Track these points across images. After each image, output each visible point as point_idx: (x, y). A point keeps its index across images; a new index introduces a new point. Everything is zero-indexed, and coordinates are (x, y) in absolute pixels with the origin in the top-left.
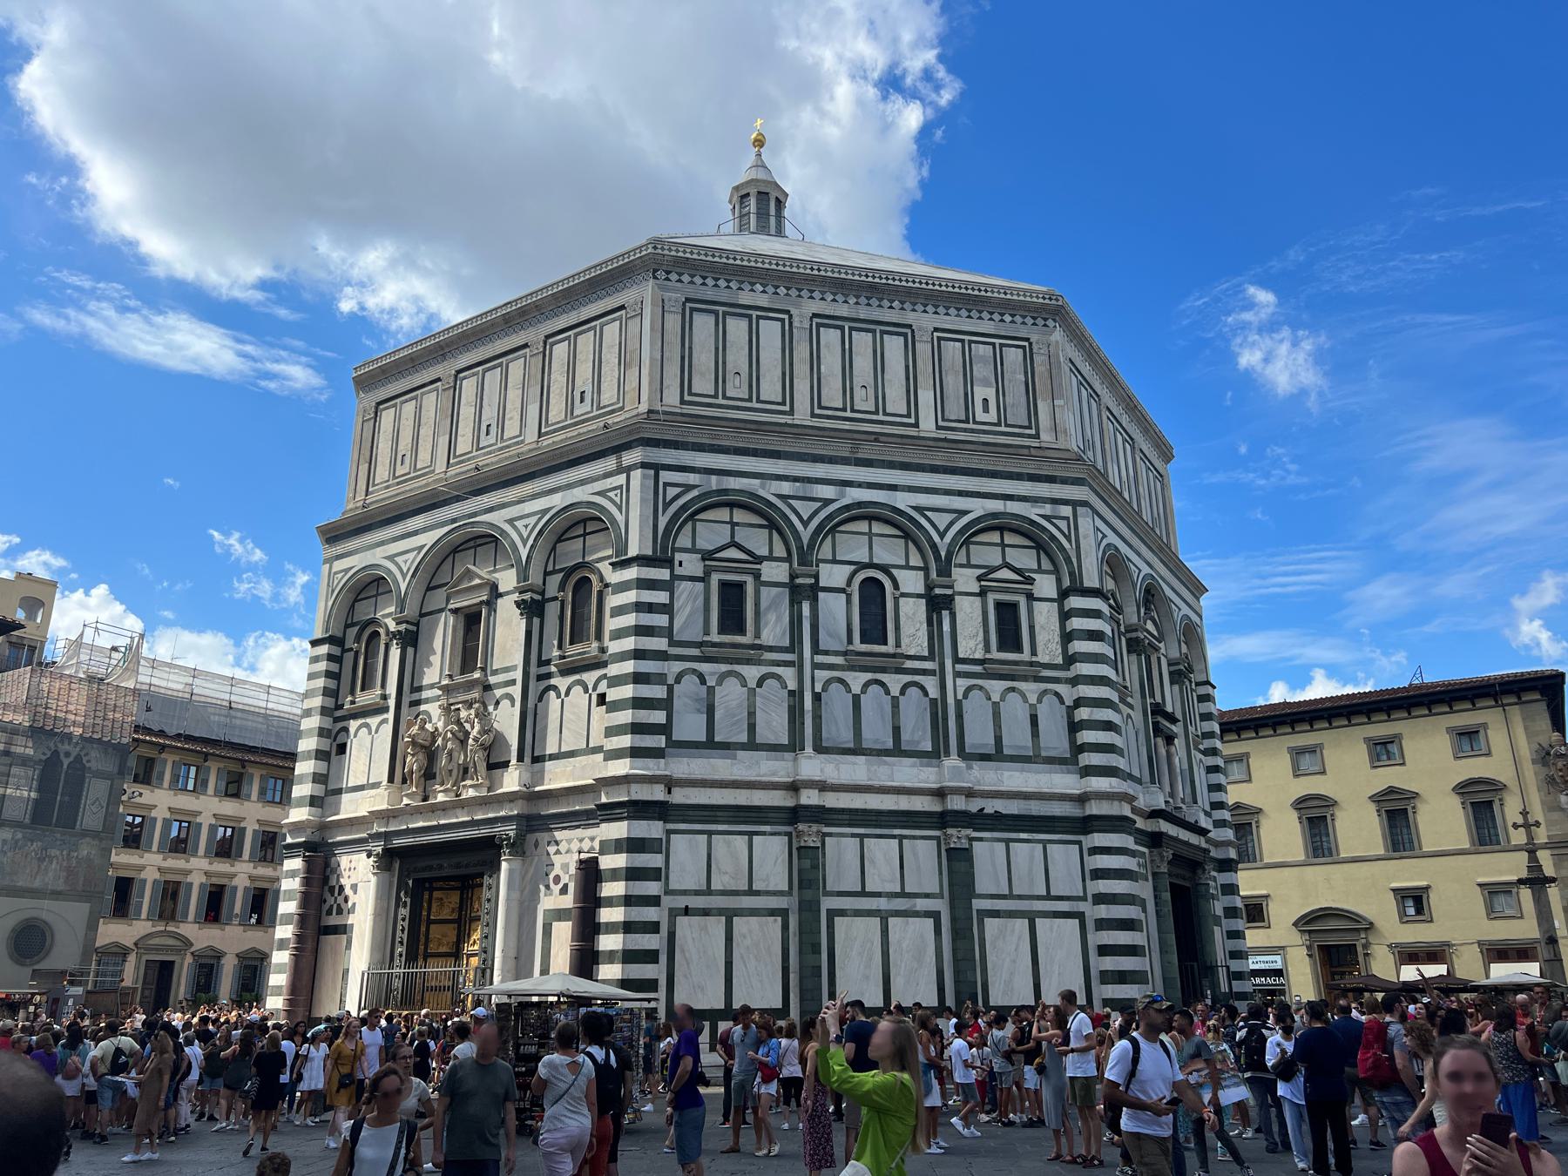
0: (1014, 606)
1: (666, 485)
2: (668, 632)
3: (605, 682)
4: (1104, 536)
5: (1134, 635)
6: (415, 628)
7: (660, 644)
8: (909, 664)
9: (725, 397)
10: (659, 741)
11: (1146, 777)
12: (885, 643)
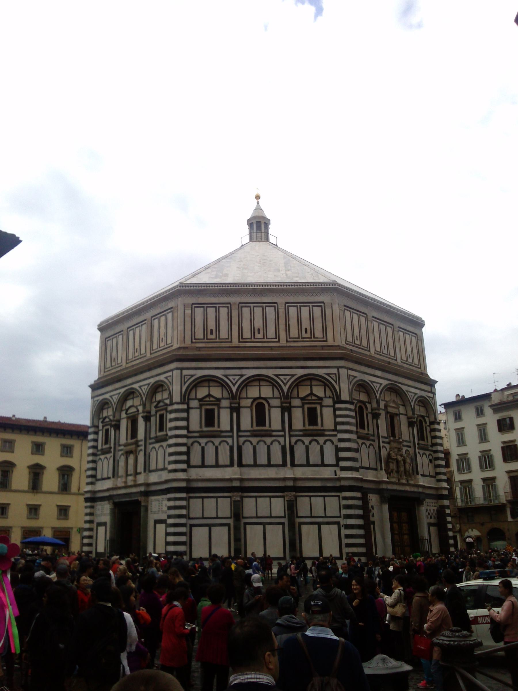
0: (315, 409)
1: (185, 376)
2: (187, 428)
3: (168, 447)
4: (355, 377)
5: (374, 412)
6: (117, 423)
7: (184, 432)
8: (274, 433)
9: (207, 339)
10: (184, 466)
11: (379, 468)
12: (264, 425)
